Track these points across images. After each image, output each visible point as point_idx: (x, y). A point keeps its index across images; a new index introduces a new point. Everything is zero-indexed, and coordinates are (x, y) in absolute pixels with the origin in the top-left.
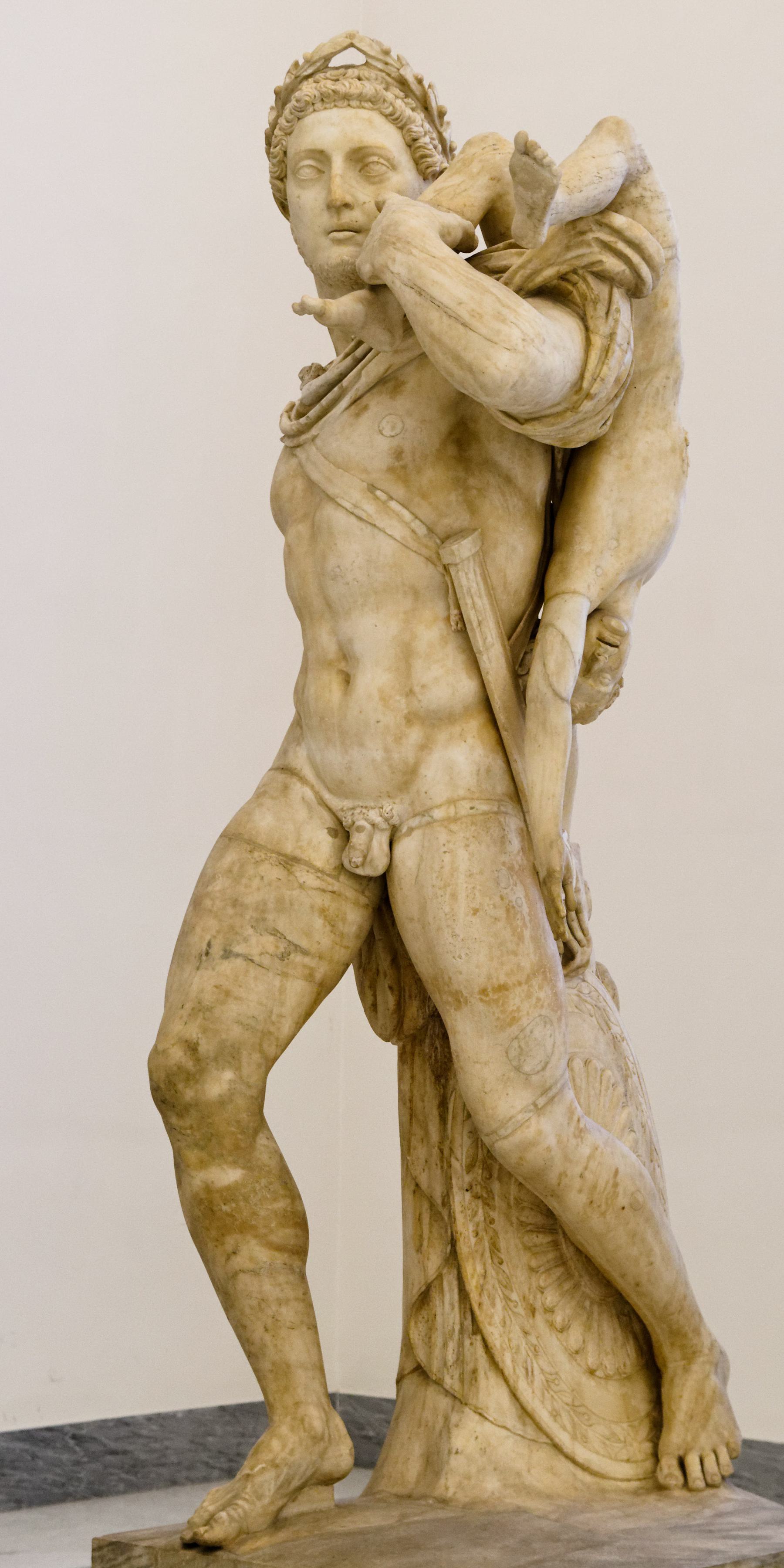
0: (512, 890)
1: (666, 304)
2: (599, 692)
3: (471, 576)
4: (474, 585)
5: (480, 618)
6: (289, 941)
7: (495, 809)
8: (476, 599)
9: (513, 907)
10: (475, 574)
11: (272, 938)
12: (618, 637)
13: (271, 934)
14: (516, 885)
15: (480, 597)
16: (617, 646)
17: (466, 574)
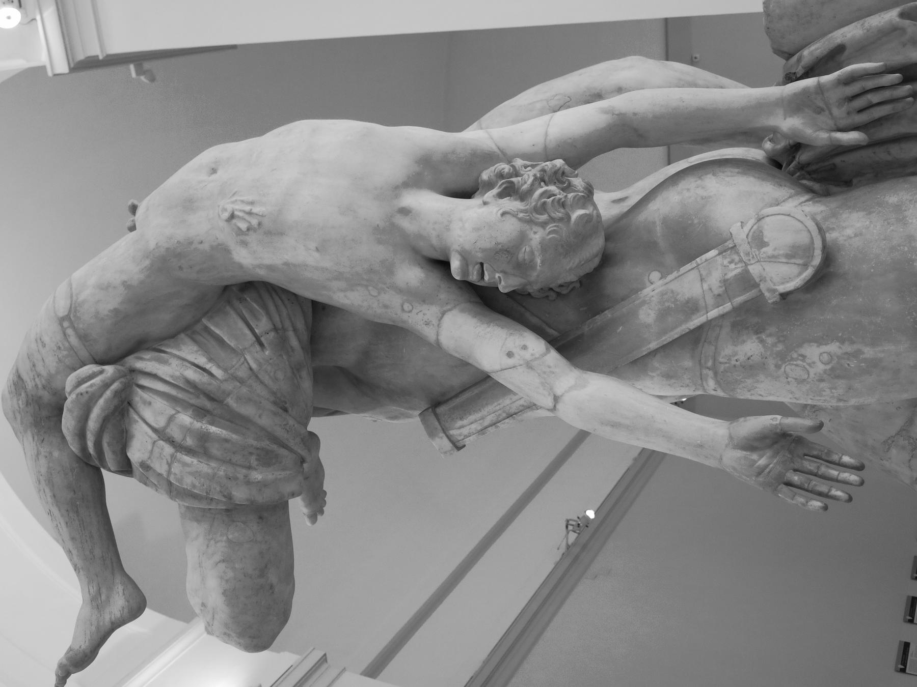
0: (809, 364)
1: (116, 311)
2: (543, 262)
3: (465, 431)
4: (473, 426)
5: (504, 415)
6: (897, 434)
7: (711, 373)
8: (487, 422)
9: (832, 369)
10: (462, 427)
11: (894, 451)
12: (471, 268)
13: (889, 449)
14: (804, 357)
15: (483, 418)
16: (482, 264)
17: (466, 437)
